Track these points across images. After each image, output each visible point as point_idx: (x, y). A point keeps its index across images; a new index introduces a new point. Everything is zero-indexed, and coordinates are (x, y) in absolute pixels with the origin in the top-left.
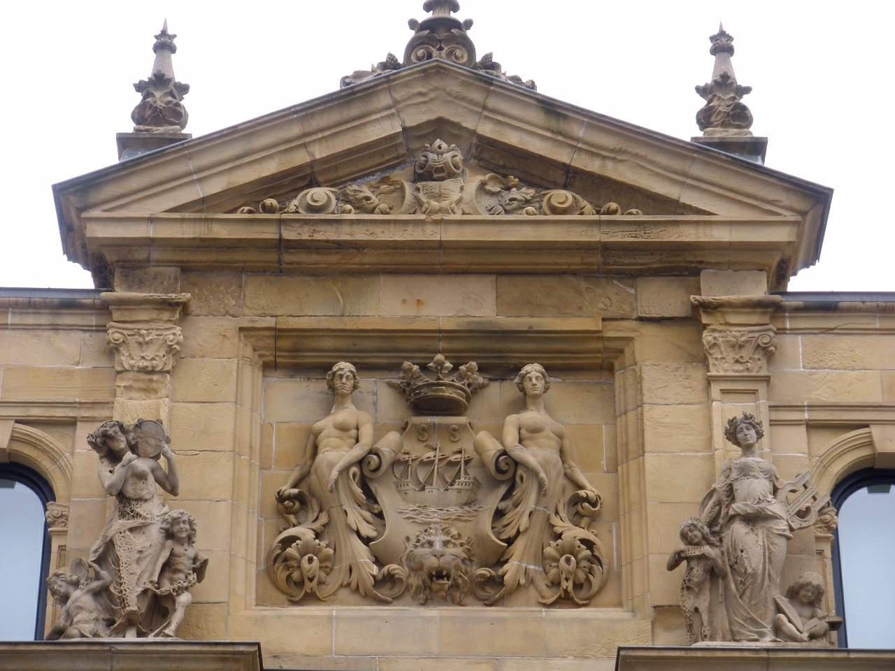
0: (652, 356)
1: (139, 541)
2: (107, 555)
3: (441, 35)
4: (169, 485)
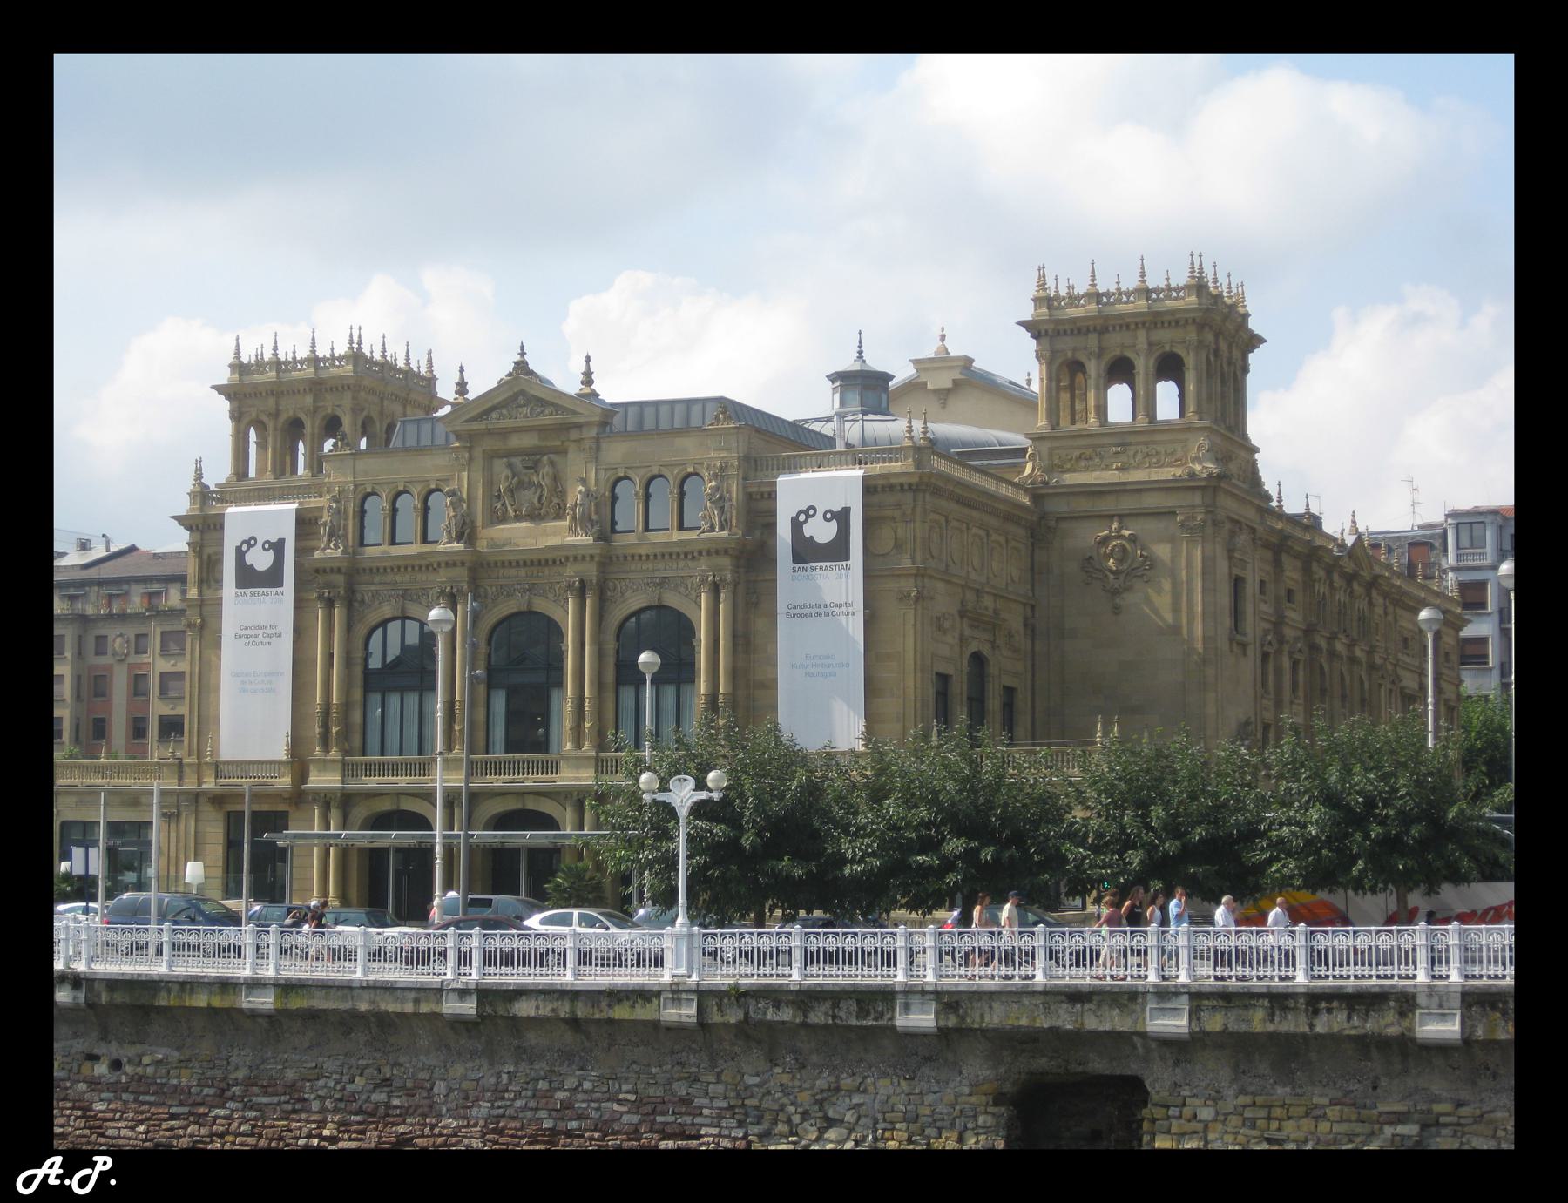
3: (521, 367)
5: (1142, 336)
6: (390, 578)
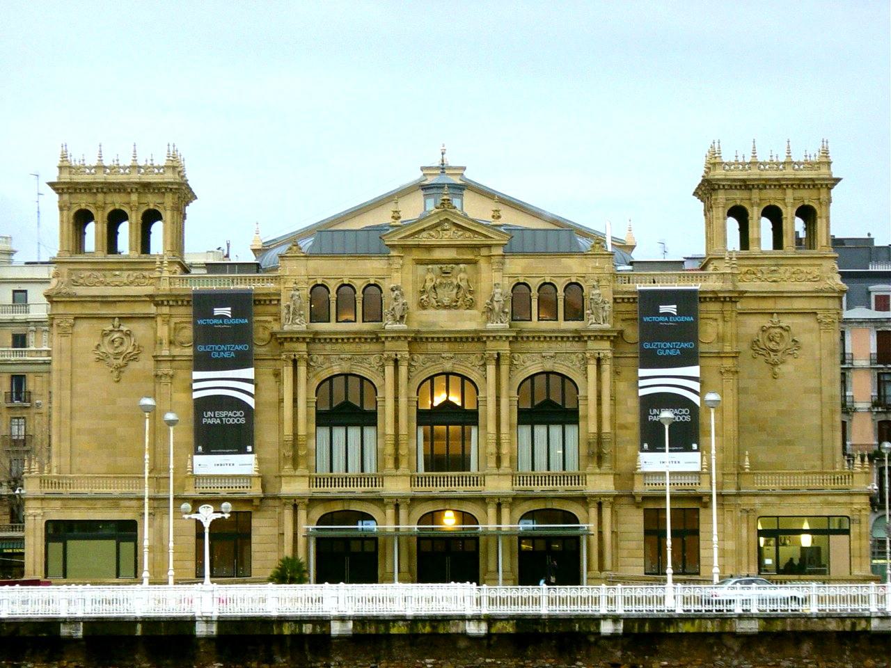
0: (483, 264)
1: (398, 307)
2: (393, 309)
4: (402, 294)
5: (789, 192)
6: (338, 347)
